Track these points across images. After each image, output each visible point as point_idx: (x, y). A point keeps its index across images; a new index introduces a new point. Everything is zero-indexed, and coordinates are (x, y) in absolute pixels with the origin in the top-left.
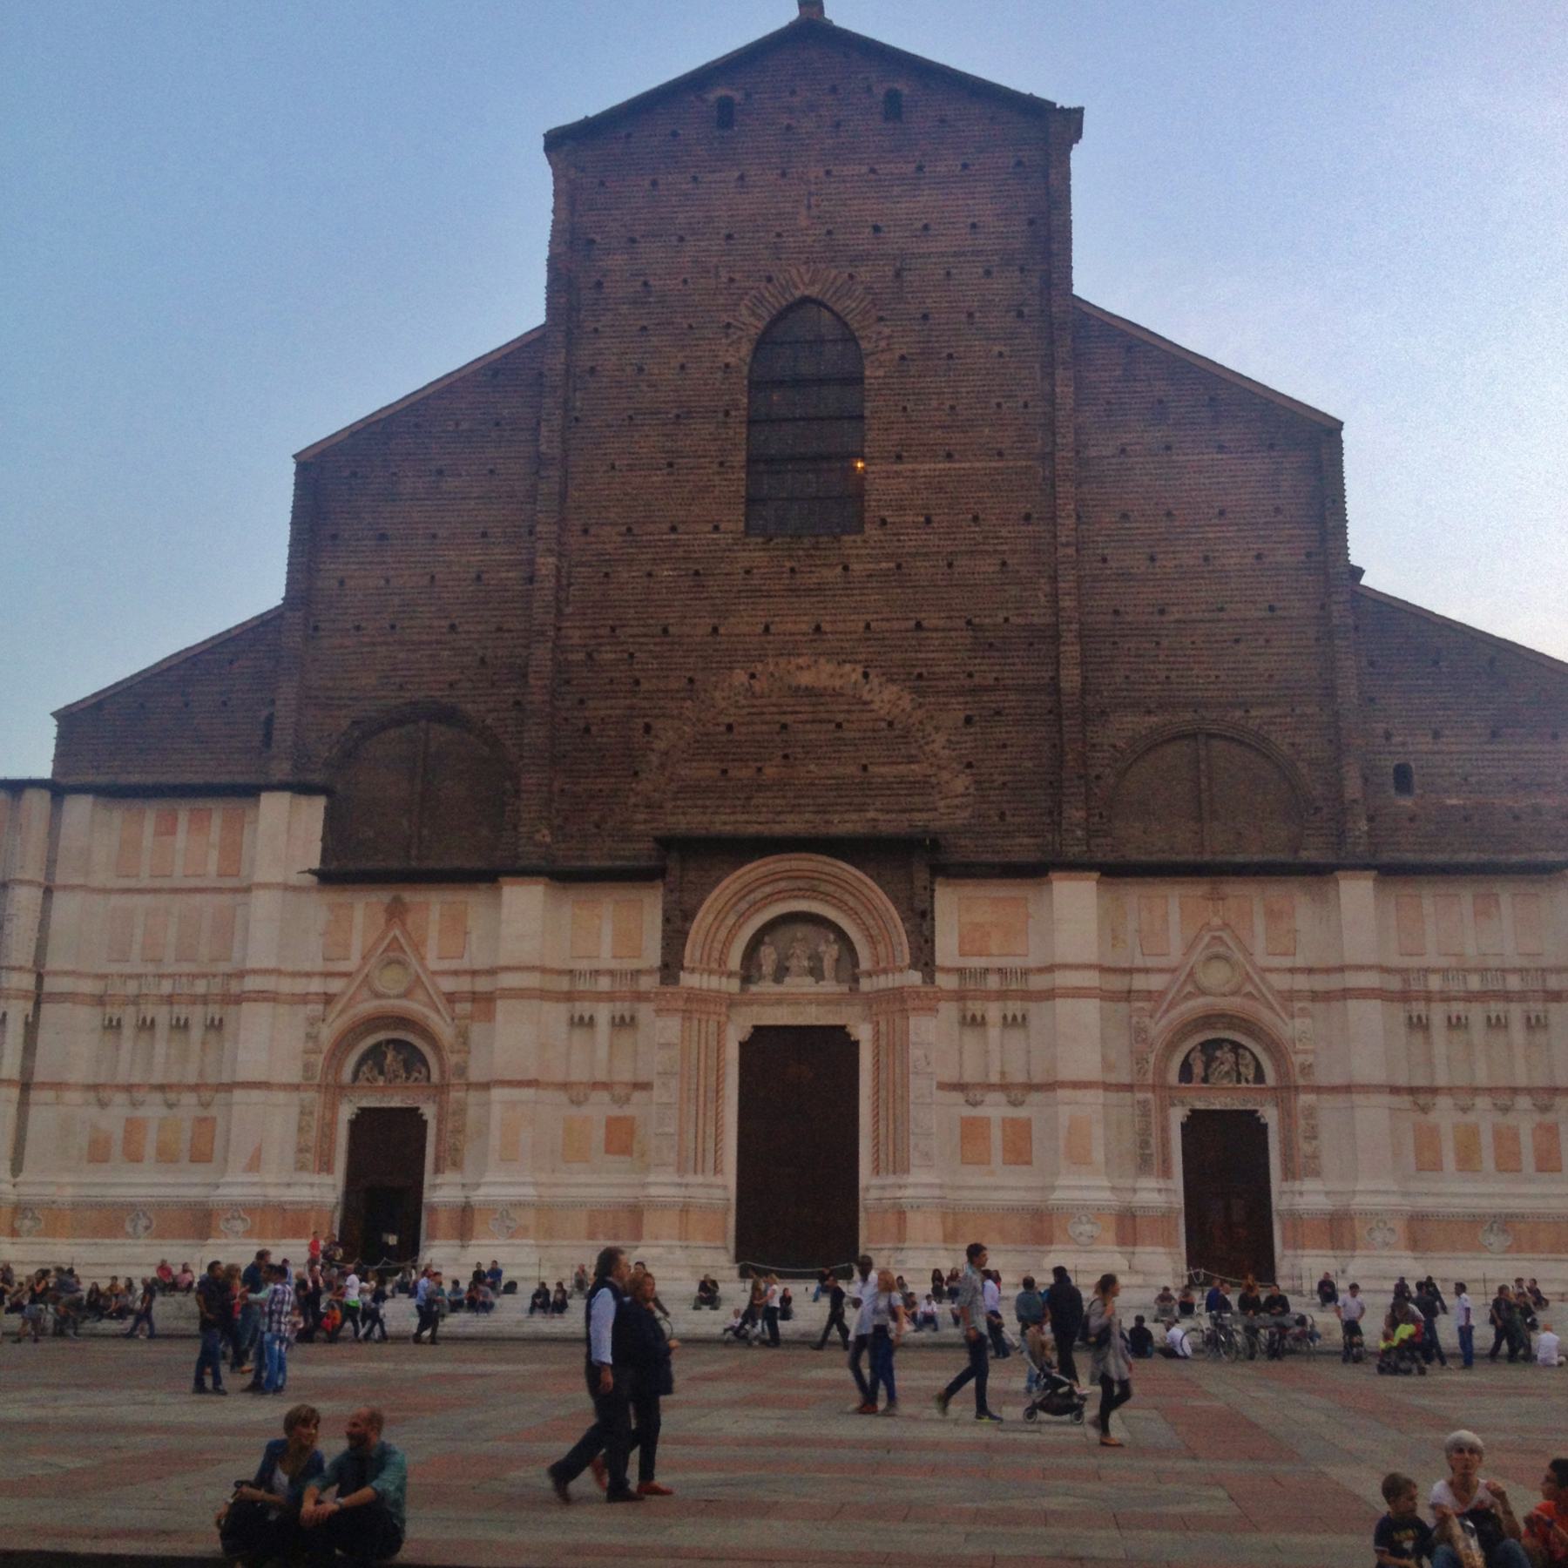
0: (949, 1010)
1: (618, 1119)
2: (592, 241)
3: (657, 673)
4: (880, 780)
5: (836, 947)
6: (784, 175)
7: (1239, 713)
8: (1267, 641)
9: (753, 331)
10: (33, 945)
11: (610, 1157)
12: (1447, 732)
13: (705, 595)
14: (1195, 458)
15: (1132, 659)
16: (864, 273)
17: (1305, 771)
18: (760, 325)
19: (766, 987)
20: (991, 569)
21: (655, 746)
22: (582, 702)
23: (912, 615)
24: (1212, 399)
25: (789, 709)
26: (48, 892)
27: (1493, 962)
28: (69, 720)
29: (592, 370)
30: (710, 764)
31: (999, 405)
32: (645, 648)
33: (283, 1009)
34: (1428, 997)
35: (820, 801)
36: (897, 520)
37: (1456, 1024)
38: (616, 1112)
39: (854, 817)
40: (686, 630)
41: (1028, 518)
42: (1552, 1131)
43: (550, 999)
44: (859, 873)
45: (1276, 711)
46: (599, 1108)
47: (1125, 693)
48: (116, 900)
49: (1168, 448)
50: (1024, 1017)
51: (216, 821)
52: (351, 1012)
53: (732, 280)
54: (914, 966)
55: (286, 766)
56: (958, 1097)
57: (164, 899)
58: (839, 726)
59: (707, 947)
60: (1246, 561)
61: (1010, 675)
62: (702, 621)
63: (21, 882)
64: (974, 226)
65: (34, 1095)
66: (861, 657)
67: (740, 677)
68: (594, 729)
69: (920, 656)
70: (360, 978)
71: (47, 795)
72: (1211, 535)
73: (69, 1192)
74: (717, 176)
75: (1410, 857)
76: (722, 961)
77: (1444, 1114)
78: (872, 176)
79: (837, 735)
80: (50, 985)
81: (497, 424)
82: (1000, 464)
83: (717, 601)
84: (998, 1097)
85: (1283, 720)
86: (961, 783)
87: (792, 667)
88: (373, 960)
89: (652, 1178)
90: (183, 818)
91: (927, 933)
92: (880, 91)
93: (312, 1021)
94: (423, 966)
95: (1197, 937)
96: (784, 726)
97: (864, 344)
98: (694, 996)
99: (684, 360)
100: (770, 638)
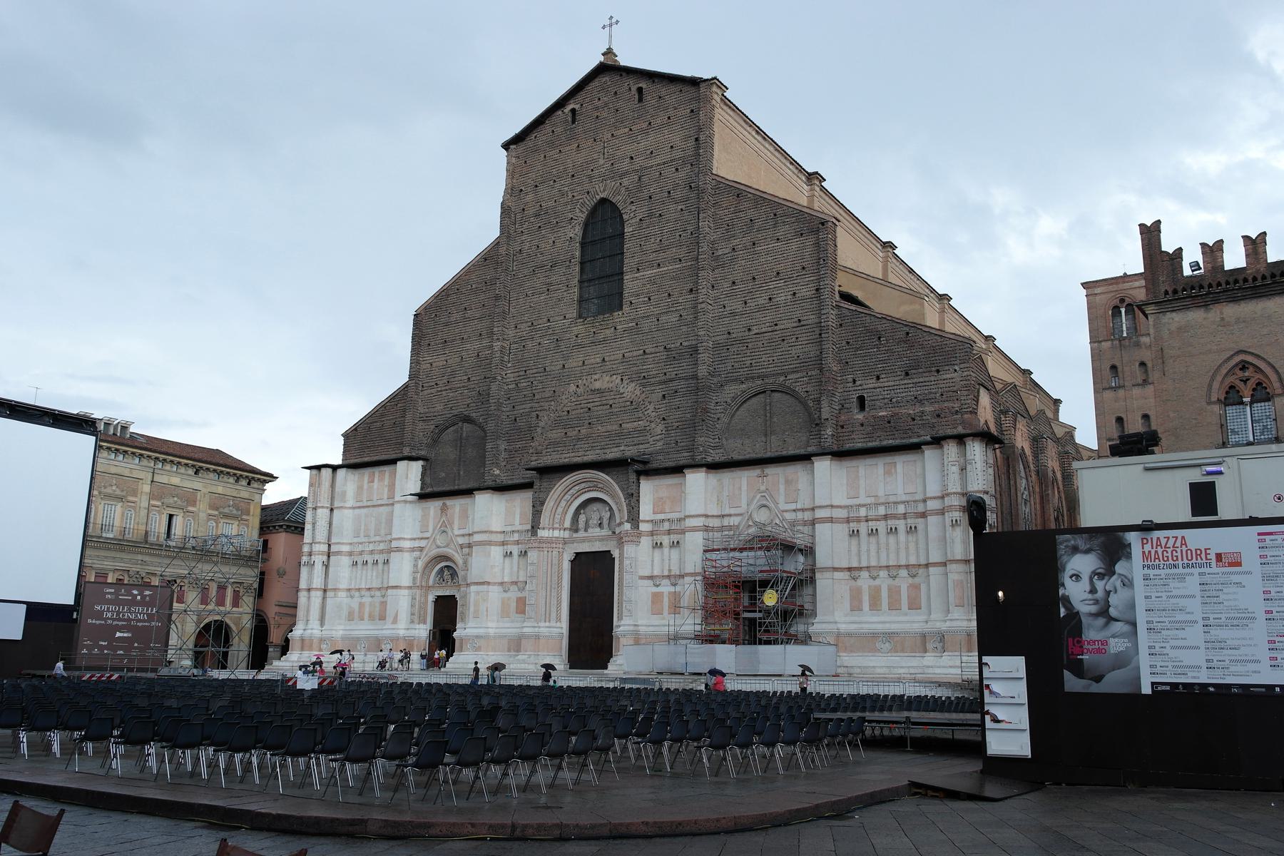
0: (646, 542)
1: (520, 598)
2: (521, 190)
3: (541, 390)
4: (625, 431)
5: (609, 513)
6: (595, 140)
7: (782, 378)
8: (797, 338)
9: (580, 219)
10: (325, 533)
11: (517, 615)
12: (883, 376)
13: (560, 350)
14: (766, 247)
15: (735, 357)
16: (626, 182)
17: (811, 405)
18: (582, 216)
19: (581, 534)
20: (674, 320)
21: (540, 425)
22: (514, 407)
23: (641, 348)
24: (775, 215)
25: (591, 401)
26: (332, 510)
27: (892, 499)
28: (346, 436)
29: (520, 250)
30: (559, 431)
31: (680, 236)
32: (537, 379)
33: (407, 555)
34: (858, 520)
35: (603, 443)
36: (637, 301)
37: (873, 533)
38: (520, 595)
39: (616, 449)
40: (553, 368)
41: (691, 290)
42: (916, 587)
43: (496, 545)
44: (607, 477)
45: (799, 375)
46: (514, 594)
47: (732, 375)
48: (357, 511)
49: (754, 244)
50: (678, 542)
51: (387, 475)
52: (429, 554)
53: (573, 196)
54: (627, 521)
55: (408, 449)
56: (650, 582)
57: (371, 509)
58: (611, 406)
59: (552, 517)
60: (789, 297)
61: (682, 372)
62: (558, 363)
63: (320, 507)
64: (672, 147)
65: (329, 594)
66: (619, 372)
67: (573, 388)
68: (518, 419)
69: (645, 367)
70: (432, 540)
71: (330, 470)
72: (772, 286)
73: (341, 632)
74: (568, 148)
75: (859, 445)
76: (562, 521)
77: (864, 581)
78: (630, 133)
79: (610, 411)
80: (334, 549)
81: (486, 283)
82: (680, 266)
83: (565, 353)
84: (666, 582)
85: (802, 379)
86: (659, 428)
87: (593, 380)
88: (436, 531)
89: (525, 624)
90: (377, 475)
91: (633, 504)
92: (634, 89)
93: (416, 559)
94: (453, 534)
95: (754, 497)
96: (589, 409)
97: (625, 217)
98: (542, 541)
99: (554, 239)
100: (585, 367)
